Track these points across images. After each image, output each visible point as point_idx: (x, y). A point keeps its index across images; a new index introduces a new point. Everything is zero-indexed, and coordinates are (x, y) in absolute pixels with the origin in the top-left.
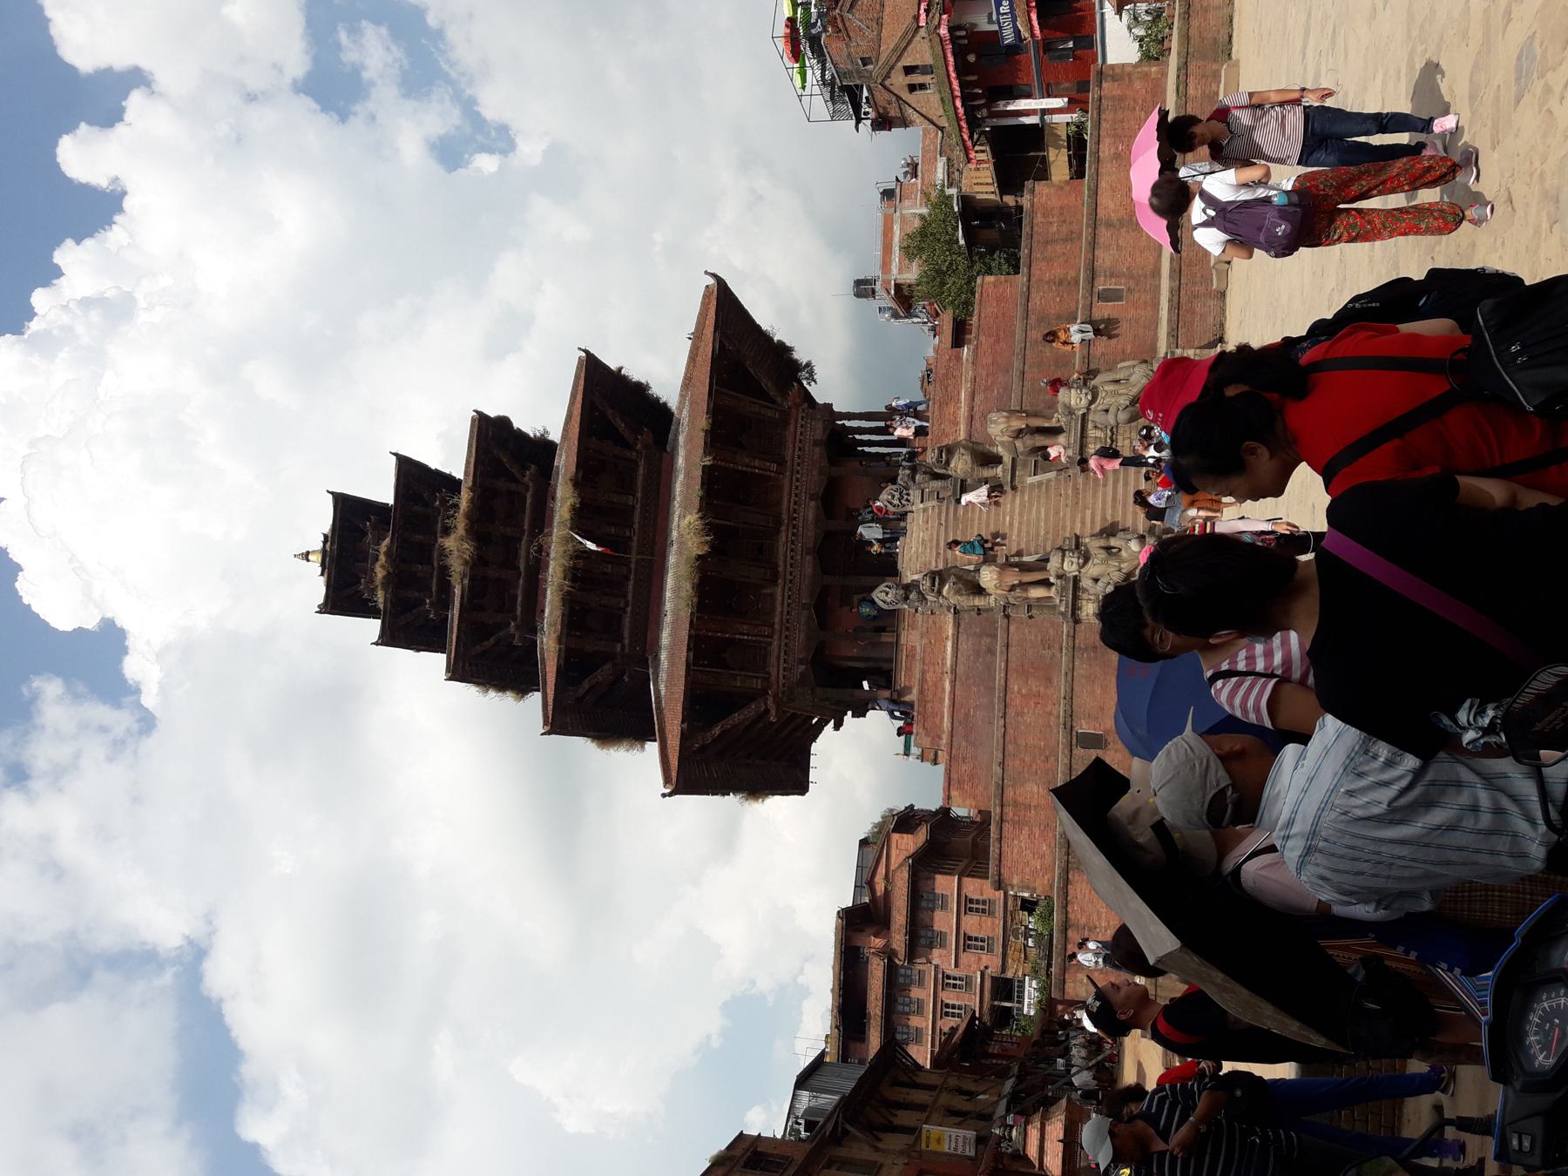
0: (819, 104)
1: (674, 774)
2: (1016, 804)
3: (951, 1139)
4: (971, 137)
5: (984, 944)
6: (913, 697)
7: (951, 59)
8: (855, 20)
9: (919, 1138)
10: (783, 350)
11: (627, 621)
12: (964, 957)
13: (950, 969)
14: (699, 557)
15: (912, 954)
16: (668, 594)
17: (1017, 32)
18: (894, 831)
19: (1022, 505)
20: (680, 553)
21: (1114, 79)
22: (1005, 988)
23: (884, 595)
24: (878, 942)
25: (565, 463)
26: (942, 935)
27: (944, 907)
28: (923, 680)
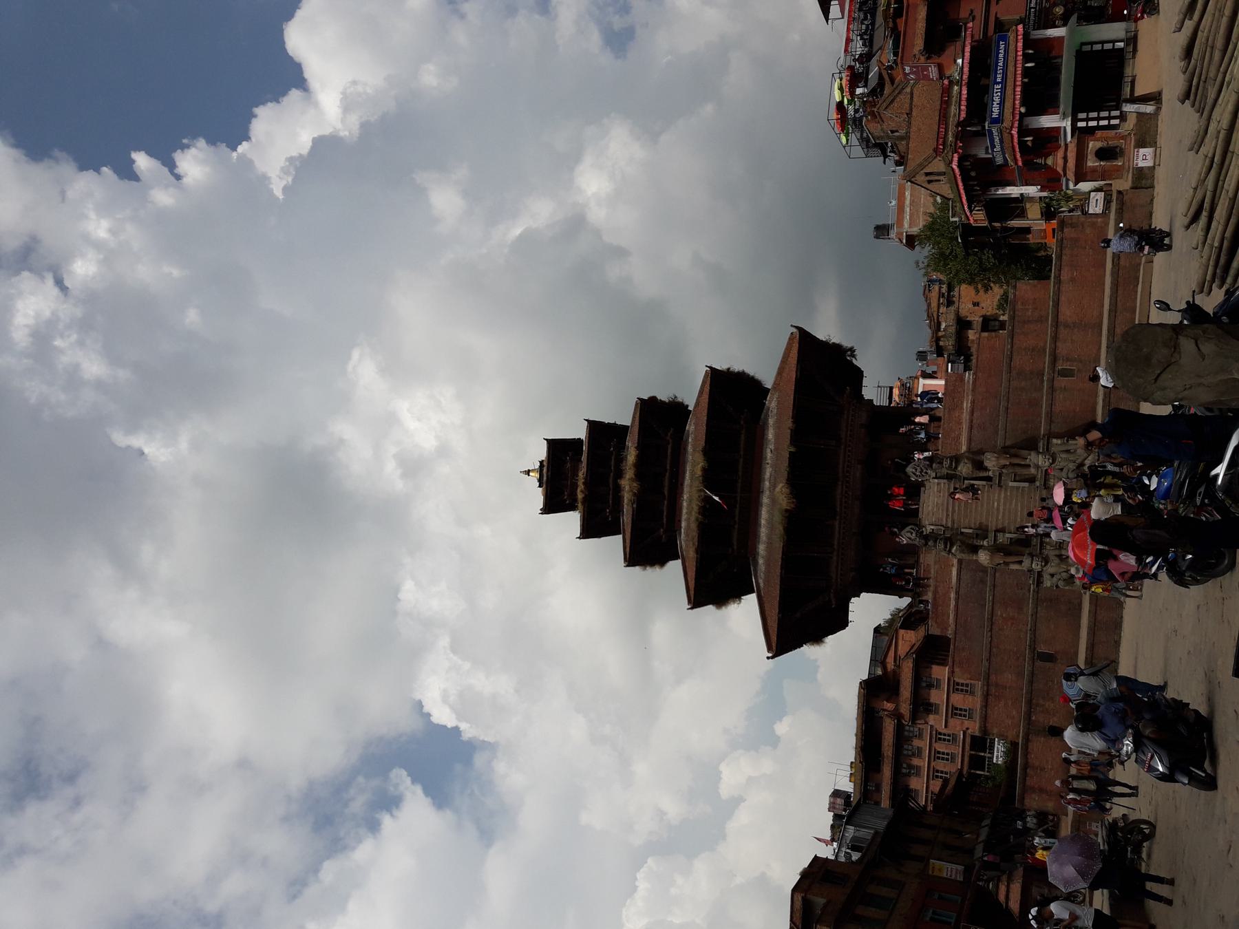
0: (858, 151)
2: (997, 685)
3: (949, 870)
4: (970, 207)
5: (966, 713)
6: (929, 596)
7: (960, 184)
8: (887, 114)
9: (927, 864)
10: (837, 348)
12: (951, 721)
14: (787, 510)
15: (915, 717)
16: (763, 522)
17: (1005, 158)
19: (1005, 497)
20: (773, 501)
21: (1072, 226)
22: (980, 743)
24: (889, 706)
25: (695, 431)
27: (938, 686)
28: (935, 593)
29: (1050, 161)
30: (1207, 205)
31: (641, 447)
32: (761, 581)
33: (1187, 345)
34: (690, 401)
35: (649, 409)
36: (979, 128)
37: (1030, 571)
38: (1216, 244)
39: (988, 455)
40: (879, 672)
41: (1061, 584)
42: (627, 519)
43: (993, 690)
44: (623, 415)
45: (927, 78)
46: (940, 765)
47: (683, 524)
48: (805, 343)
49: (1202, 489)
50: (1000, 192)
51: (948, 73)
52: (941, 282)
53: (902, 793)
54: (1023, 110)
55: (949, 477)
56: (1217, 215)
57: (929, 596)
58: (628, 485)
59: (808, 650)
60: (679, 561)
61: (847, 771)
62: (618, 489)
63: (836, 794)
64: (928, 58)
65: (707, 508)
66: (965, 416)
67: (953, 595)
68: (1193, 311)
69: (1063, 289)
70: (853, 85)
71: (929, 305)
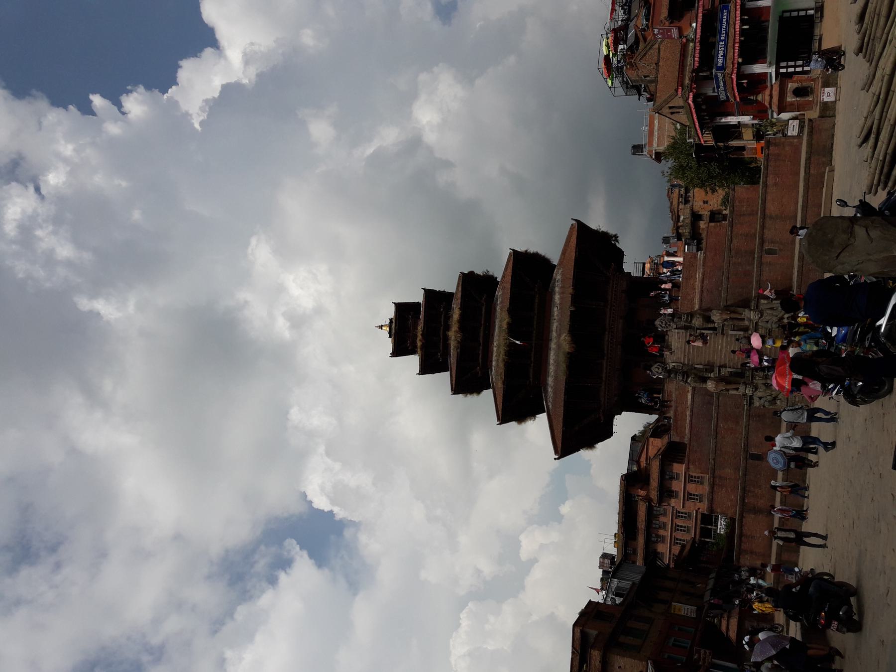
1: (559, 449)
3: (686, 610)
6: (671, 414)
8: (641, 64)
11: (531, 371)
13: (680, 508)
14: (568, 353)
15: (660, 501)
16: (551, 361)
17: (727, 97)
18: (651, 436)
20: (559, 346)
21: (776, 145)
22: (708, 519)
23: (657, 372)
24: (642, 493)
25: (502, 296)
26: (677, 492)
27: (678, 478)
28: (676, 411)
29: (760, 98)
30: (874, 130)
31: (463, 308)
32: (550, 404)
33: (860, 231)
34: (499, 274)
35: (468, 280)
36: (708, 73)
37: (745, 395)
38: (881, 158)
39: (714, 312)
40: (635, 469)
41: (766, 404)
42: (453, 360)
43: (717, 480)
44: (450, 285)
45: (670, 37)
46: (679, 535)
47: (494, 363)
48: (582, 232)
49: (870, 336)
50: (723, 120)
51: (685, 34)
52: (680, 186)
53: (652, 555)
54: (740, 60)
55: (686, 328)
56: (881, 137)
57: (671, 414)
58: (453, 335)
59: (584, 453)
60: (491, 390)
61: (613, 540)
62: (446, 339)
63: (605, 556)
64: (671, 23)
65: (511, 352)
66: (698, 284)
67: (688, 413)
68: (864, 207)
69: (769, 191)
70: (616, 42)
71: (671, 203)
